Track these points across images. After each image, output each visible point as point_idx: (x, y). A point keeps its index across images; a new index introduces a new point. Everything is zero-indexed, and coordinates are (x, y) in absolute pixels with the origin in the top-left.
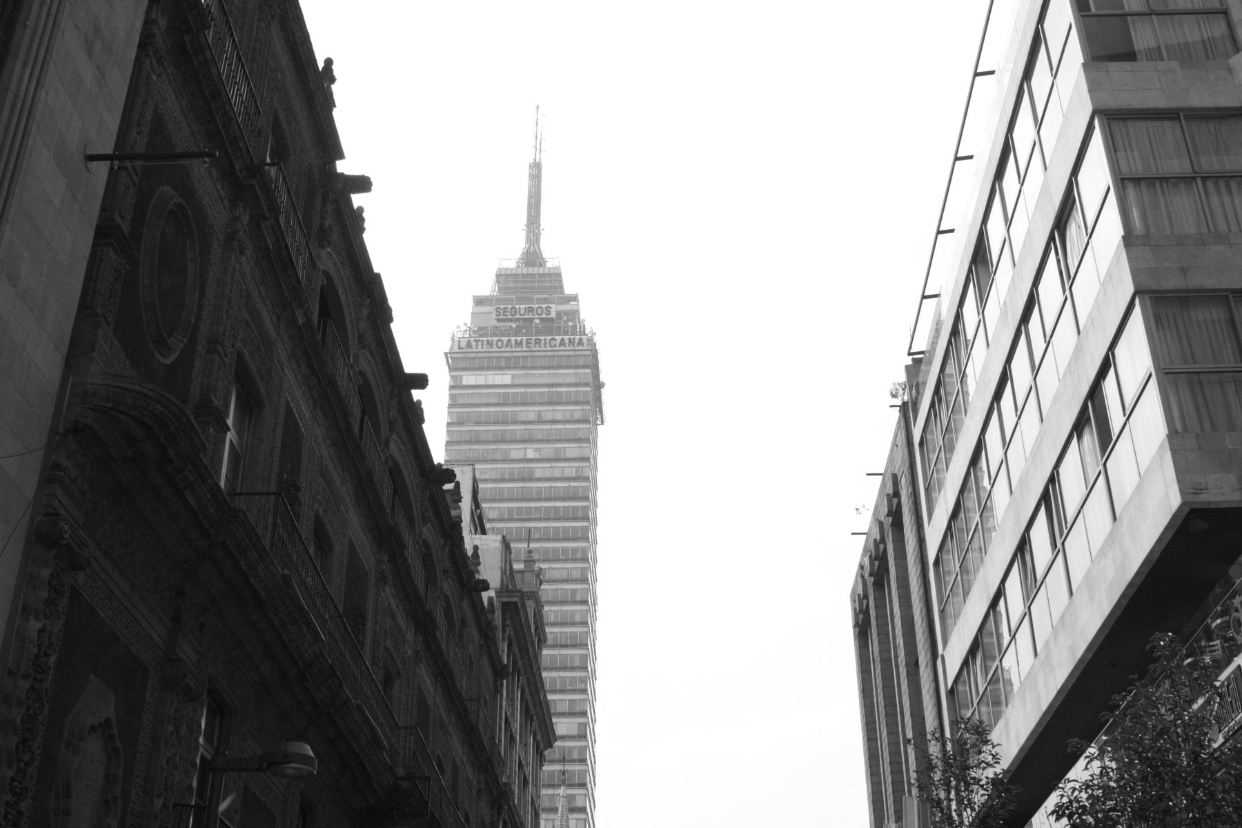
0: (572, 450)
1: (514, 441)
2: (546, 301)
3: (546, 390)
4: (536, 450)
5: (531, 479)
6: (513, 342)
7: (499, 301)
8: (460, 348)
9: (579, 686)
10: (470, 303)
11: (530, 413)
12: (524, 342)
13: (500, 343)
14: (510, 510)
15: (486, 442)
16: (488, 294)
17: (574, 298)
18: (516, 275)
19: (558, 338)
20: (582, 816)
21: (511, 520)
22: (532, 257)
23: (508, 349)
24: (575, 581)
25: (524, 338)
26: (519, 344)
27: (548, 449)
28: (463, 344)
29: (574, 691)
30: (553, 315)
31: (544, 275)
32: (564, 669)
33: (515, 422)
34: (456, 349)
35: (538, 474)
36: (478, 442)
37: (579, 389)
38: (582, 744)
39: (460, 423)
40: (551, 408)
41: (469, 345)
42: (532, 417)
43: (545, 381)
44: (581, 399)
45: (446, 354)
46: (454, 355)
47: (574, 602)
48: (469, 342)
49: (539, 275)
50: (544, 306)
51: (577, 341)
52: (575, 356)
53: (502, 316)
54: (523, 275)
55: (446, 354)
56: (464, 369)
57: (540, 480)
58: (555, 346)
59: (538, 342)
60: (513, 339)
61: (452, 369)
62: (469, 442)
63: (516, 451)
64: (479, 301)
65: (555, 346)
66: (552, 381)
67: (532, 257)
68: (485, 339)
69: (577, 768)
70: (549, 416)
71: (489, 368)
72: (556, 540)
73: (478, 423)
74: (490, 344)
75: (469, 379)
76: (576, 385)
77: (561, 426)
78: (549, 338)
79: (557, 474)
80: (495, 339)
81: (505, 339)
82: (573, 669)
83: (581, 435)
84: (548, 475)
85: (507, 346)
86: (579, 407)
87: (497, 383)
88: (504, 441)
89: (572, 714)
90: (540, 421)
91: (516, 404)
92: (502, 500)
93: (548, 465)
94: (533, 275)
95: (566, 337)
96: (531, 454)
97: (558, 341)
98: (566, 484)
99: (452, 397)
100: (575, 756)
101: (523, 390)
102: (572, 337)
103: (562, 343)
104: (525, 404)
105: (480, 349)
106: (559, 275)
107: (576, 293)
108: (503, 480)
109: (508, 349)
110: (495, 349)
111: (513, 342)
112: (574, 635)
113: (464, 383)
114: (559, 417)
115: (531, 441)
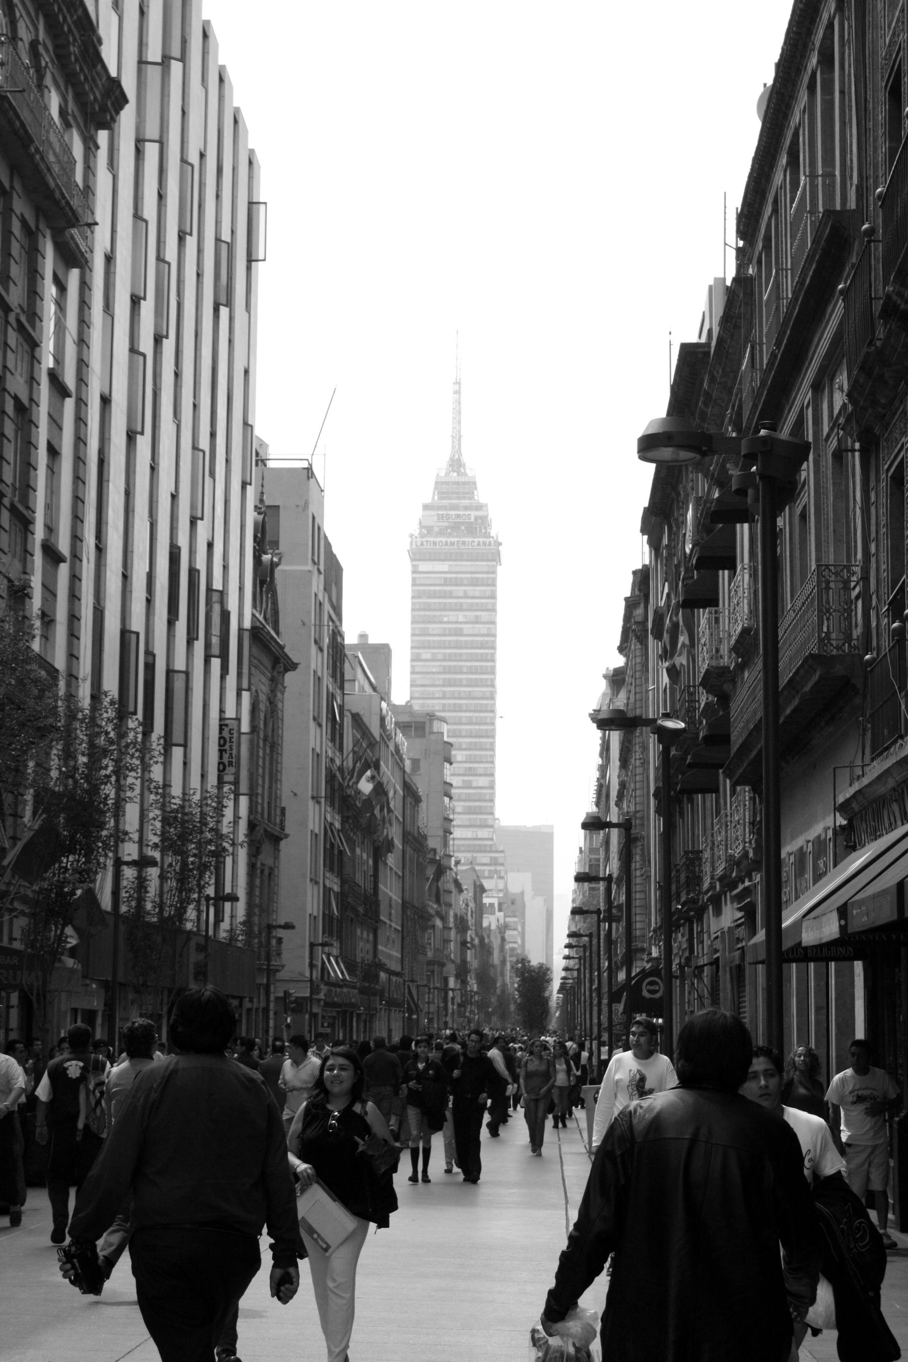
0: (484, 615)
1: (451, 610)
2: (466, 508)
3: (469, 576)
4: (465, 616)
5: (462, 635)
7: (439, 508)
9: (490, 760)
10: (421, 507)
11: (459, 590)
14: (450, 654)
15: (434, 610)
17: (486, 505)
18: (447, 483)
19: (476, 540)
20: (491, 830)
21: (450, 660)
22: (456, 464)
24: (487, 699)
25: (456, 540)
26: (452, 544)
27: (471, 615)
28: (419, 544)
29: (486, 762)
30: (473, 519)
31: (465, 483)
32: (481, 749)
33: (451, 597)
34: (414, 546)
35: (465, 632)
36: (430, 610)
39: (419, 597)
40: (472, 588)
41: (422, 544)
42: (461, 594)
43: (469, 569)
47: (487, 711)
50: (467, 513)
53: (441, 518)
56: (419, 560)
57: (467, 635)
59: (464, 543)
60: (449, 540)
61: (412, 560)
62: (425, 610)
63: (452, 616)
64: (426, 507)
66: (473, 570)
67: (456, 464)
68: (431, 539)
69: (489, 804)
70: (471, 594)
71: (435, 560)
72: (476, 673)
73: (429, 597)
74: (435, 543)
75: (424, 566)
76: (487, 573)
77: (478, 601)
78: (471, 540)
79: (477, 632)
80: (438, 540)
81: (444, 540)
82: (486, 749)
83: (490, 607)
84: (471, 632)
86: (489, 588)
87: (441, 570)
88: (445, 610)
89: (486, 775)
90: (466, 596)
91: (451, 585)
92: (445, 648)
93: (471, 626)
95: (481, 540)
96: (461, 619)
97: (476, 544)
98: (481, 639)
99: (414, 579)
101: (455, 575)
102: (484, 540)
103: (479, 544)
104: (456, 585)
106: (475, 483)
108: (445, 635)
112: (487, 730)
114: (477, 594)
115: (461, 610)
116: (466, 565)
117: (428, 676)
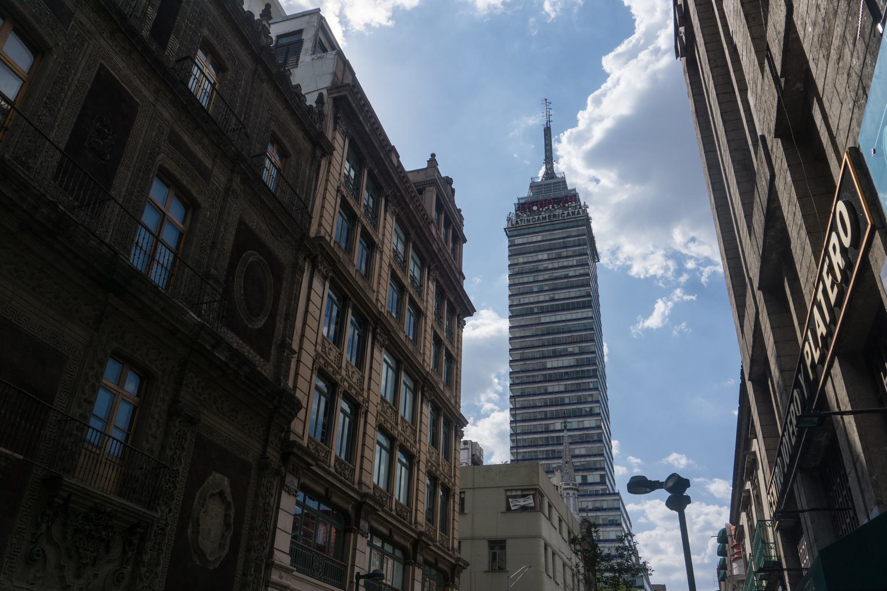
3: (562, 241)
6: (541, 218)
8: (512, 225)
12: (547, 217)
13: (534, 220)
16: (526, 195)
20: (603, 473)
22: (550, 174)
23: (539, 222)
26: (544, 218)
28: (514, 223)
37: (580, 238)
38: (600, 431)
40: (565, 250)
44: (582, 243)
45: (505, 229)
46: (510, 229)
48: (517, 221)
49: (554, 183)
51: (576, 212)
52: (577, 221)
54: (545, 185)
55: (505, 229)
56: (516, 236)
58: (564, 217)
59: (555, 216)
61: (509, 237)
65: (564, 217)
67: (550, 174)
70: (564, 254)
75: (519, 240)
80: (531, 218)
81: (536, 217)
85: (538, 220)
94: (550, 184)
100: (596, 438)
105: (523, 224)
107: (574, 188)
109: (539, 222)
110: (531, 223)
111: (541, 218)
113: (516, 243)
116: (558, 234)
117: (526, 328)
